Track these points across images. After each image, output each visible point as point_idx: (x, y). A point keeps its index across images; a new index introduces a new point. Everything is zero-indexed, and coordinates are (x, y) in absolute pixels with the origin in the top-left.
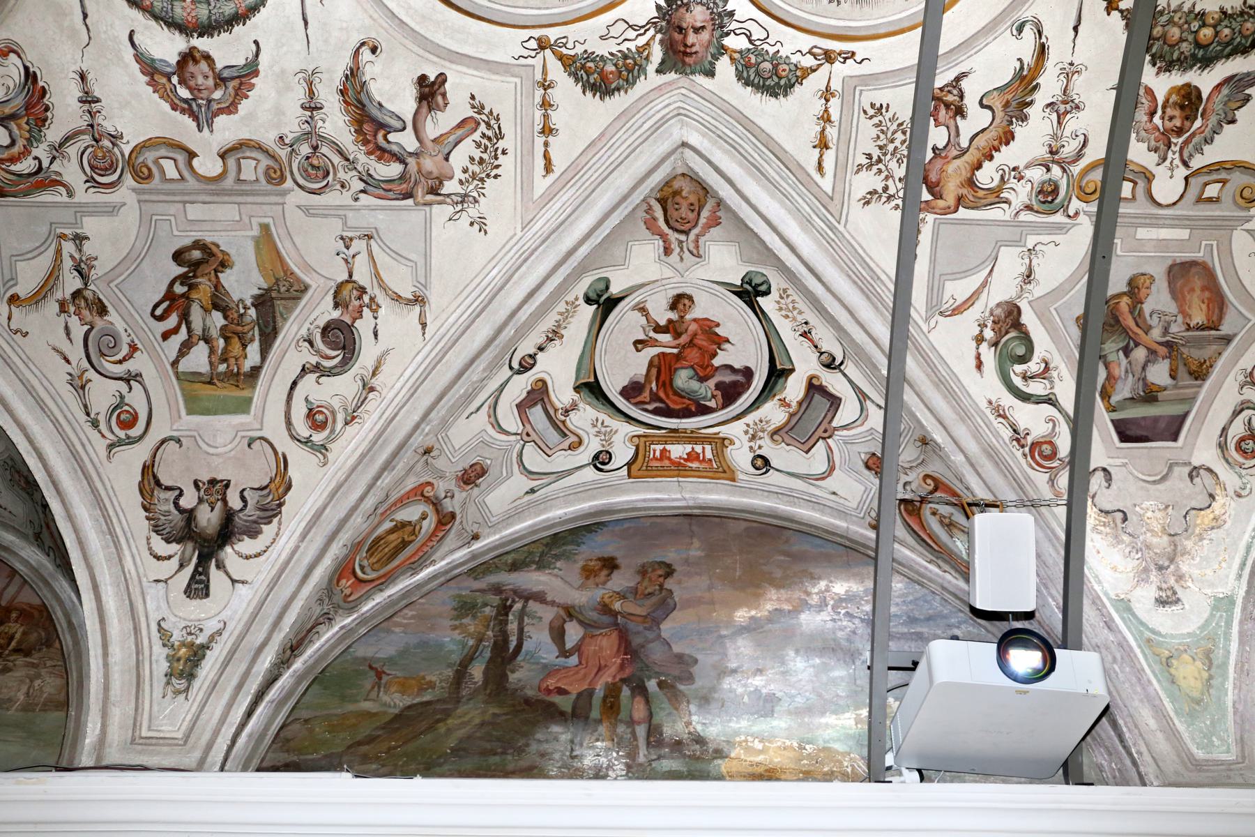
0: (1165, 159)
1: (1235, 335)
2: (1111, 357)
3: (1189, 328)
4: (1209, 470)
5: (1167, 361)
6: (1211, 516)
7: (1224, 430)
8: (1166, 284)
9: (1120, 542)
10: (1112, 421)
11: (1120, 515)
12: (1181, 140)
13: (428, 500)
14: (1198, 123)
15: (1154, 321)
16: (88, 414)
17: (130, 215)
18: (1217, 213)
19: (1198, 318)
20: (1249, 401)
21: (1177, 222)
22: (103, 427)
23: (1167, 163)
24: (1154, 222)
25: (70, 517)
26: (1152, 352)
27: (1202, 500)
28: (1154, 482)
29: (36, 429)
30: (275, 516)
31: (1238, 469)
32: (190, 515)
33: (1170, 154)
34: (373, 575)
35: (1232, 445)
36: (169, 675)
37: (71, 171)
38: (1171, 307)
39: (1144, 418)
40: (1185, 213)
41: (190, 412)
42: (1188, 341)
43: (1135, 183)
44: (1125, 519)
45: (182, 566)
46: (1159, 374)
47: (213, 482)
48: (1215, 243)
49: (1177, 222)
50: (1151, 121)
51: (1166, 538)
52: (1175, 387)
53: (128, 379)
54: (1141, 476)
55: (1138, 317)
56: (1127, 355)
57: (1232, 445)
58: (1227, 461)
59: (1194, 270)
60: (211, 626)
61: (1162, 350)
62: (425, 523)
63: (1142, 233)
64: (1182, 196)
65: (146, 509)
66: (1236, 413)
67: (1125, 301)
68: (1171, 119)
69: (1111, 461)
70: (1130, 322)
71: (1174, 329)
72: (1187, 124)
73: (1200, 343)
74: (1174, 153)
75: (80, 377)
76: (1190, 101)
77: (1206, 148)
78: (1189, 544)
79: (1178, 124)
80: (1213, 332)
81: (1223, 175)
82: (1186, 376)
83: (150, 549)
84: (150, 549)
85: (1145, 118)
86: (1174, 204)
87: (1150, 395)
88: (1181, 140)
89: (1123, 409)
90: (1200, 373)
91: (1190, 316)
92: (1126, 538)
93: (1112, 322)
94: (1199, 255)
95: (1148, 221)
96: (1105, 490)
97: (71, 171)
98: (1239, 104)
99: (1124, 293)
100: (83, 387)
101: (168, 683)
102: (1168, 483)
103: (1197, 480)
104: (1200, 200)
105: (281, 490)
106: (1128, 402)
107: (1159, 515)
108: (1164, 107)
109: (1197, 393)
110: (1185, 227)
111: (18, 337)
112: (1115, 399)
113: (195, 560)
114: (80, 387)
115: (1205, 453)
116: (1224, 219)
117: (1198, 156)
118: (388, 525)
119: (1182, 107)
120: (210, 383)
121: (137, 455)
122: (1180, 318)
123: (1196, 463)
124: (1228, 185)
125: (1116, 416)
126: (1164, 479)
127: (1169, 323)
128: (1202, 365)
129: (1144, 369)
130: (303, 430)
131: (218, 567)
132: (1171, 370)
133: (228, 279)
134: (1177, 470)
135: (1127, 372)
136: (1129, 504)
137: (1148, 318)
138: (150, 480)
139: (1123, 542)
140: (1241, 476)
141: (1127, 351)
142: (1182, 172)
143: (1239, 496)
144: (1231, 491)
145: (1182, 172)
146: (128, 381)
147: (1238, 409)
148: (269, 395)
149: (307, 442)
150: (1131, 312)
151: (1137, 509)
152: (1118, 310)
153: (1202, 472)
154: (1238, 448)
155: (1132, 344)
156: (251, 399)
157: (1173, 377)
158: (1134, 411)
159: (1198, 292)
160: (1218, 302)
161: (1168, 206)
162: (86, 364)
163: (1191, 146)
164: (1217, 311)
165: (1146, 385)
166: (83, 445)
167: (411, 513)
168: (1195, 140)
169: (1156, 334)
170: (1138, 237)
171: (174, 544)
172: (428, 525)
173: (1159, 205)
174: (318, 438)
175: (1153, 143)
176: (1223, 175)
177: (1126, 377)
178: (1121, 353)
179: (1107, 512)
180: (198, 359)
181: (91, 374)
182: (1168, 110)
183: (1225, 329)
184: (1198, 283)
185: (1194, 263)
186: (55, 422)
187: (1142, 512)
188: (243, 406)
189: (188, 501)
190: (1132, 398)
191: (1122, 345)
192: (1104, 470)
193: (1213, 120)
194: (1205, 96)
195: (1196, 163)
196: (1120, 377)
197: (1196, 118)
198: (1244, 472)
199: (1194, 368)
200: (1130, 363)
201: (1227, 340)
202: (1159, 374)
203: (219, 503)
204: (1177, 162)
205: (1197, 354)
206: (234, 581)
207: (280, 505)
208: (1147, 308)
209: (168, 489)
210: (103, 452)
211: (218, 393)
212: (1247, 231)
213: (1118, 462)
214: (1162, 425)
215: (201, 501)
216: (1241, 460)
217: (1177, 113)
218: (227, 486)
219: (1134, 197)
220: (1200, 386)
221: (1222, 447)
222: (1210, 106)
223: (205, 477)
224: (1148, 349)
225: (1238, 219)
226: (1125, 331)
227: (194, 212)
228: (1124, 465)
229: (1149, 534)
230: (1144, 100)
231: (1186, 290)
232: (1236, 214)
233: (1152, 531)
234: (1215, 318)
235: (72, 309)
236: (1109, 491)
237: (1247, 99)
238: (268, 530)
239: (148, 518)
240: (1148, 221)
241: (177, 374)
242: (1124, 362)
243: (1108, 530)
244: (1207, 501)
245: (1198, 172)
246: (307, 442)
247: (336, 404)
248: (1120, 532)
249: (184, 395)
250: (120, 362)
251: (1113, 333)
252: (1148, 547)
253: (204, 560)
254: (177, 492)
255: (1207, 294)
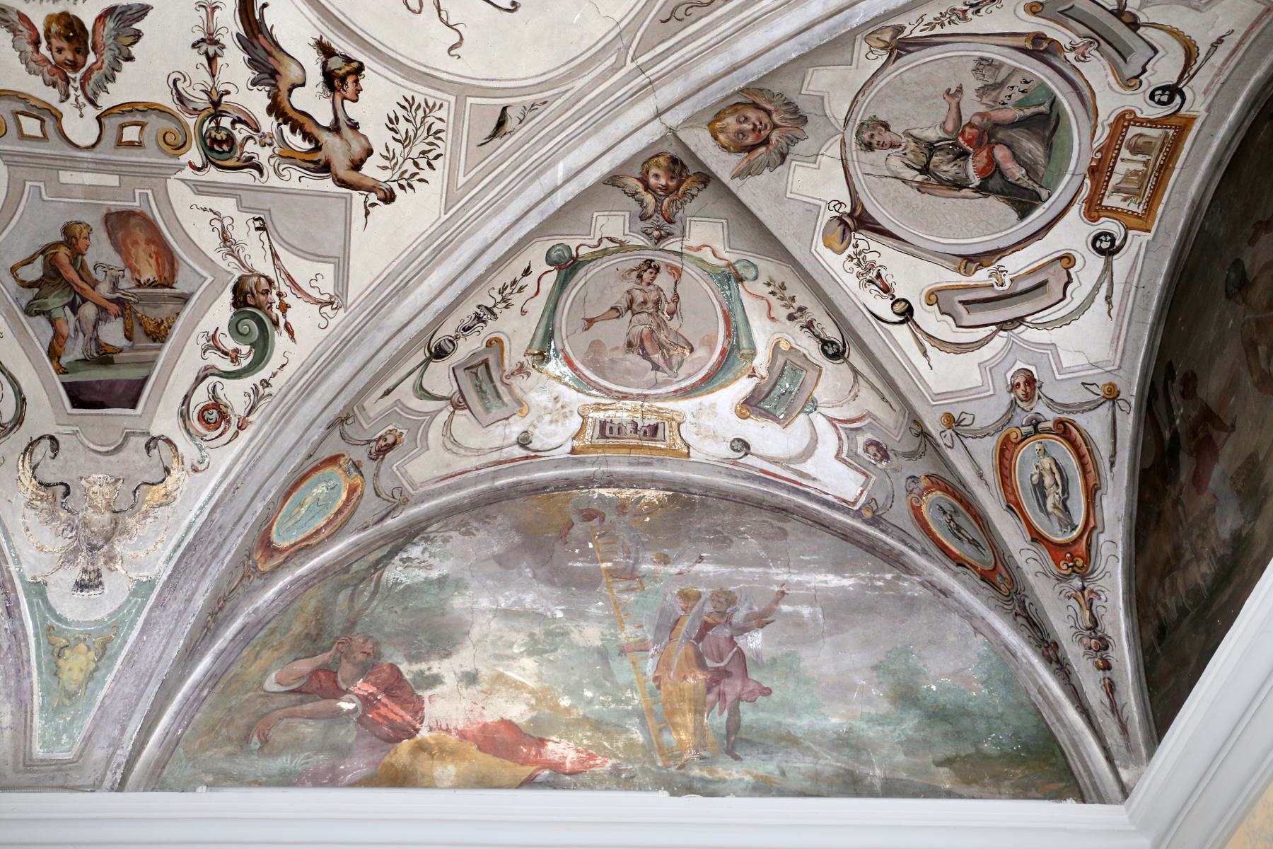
0: (68, 96)
1: (192, 294)
2: (57, 313)
3: (139, 285)
4: (168, 441)
5: (120, 321)
6: (163, 492)
7: (187, 398)
8: (104, 235)
9: (53, 516)
10: (63, 384)
11: (62, 488)
12: (78, 75)
14: (91, 58)
15: (100, 276)
18: (144, 159)
19: (148, 274)
20: (213, 367)
21: (101, 167)
23: (72, 98)
24: (74, 165)
26: (101, 309)
27: (158, 474)
28: (107, 453)
31: (198, 441)
33: (72, 91)
35: (194, 415)
38: (116, 261)
39: (99, 382)
40: (107, 157)
42: (141, 299)
43: (43, 121)
44: (67, 493)
46: (112, 333)
48: (149, 192)
49: (102, 167)
50: (38, 52)
51: (108, 515)
52: (132, 348)
54: (92, 446)
55: (82, 270)
56: (74, 312)
57: (194, 415)
58: (188, 432)
59: (133, 221)
61: (114, 308)
63: (66, 177)
64: (99, 138)
66: (199, 380)
67: (63, 253)
68: (60, 50)
69: (60, 429)
70: (72, 275)
71: (123, 284)
72: (80, 58)
73: (155, 302)
74: (76, 89)
76: (74, 31)
77: (110, 86)
78: (131, 522)
79: (70, 57)
80: (167, 290)
81: (139, 118)
82: (143, 337)
85: (30, 48)
86: (93, 146)
87: (104, 357)
88: (78, 75)
89: (75, 371)
90: (158, 334)
91: (139, 272)
92: (63, 514)
93: (52, 274)
94: (135, 205)
95: (68, 164)
96: (49, 460)
98: (130, 40)
99: (61, 243)
102: (122, 454)
103: (154, 452)
104: (120, 143)
106: (80, 364)
107: (106, 489)
108: (48, 38)
109: (157, 356)
110: (112, 173)
112: (65, 360)
115: (165, 422)
116: (153, 165)
117: (103, 94)
119: (68, 39)
122: (128, 273)
123: (155, 433)
124: (147, 129)
125: (69, 378)
126: (118, 449)
127: (117, 278)
128: (159, 325)
129: (95, 327)
132: (126, 330)
134: (133, 439)
135: (76, 330)
136: (74, 476)
137: (93, 272)
139: (59, 518)
140: (200, 449)
141: (74, 308)
142: (91, 112)
143: (195, 470)
144: (188, 466)
145: (91, 112)
147: (202, 375)
150: (73, 264)
151: (83, 482)
152: (56, 261)
153: (160, 443)
154: (201, 417)
155: (78, 299)
157: (129, 338)
158: (87, 373)
159: (143, 245)
160: (167, 258)
161: (87, 148)
163: (91, 82)
164: (167, 267)
165: (99, 345)
168: (95, 76)
169: (104, 289)
170: (63, 180)
173: (77, 147)
175: (48, 77)
176: (139, 118)
177: (77, 337)
178: (67, 309)
179: (47, 486)
182: (53, 40)
183: (181, 287)
184: (141, 236)
185: (131, 214)
187: (87, 486)
190: (85, 360)
191: (67, 300)
192: (52, 438)
193: (107, 56)
194: (89, 27)
195: (105, 101)
196: (69, 335)
197: (88, 52)
198: (205, 444)
199: (151, 328)
200: (79, 320)
201: (184, 299)
202: (112, 333)
204: (82, 99)
205: (154, 314)
208: (90, 259)
212: (183, 180)
213: (68, 429)
214: (120, 390)
216: (203, 431)
217: (64, 44)
219: (45, 135)
220: (160, 349)
221: (184, 416)
222: (99, 39)
224: (97, 306)
225: (169, 167)
226: (69, 285)
228: (75, 433)
229: (91, 510)
230: (21, 28)
231: (129, 241)
232: (164, 161)
233: (96, 506)
234: (167, 275)
236: (55, 462)
237: (138, 35)
240: (68, 164)
242: (72, 319)
243: (45, 505)
244: (160, 474)
245: (109, 112)
248: (58, 507)
251: (56, 286)
252: (86, 525)
255: (153, 248)
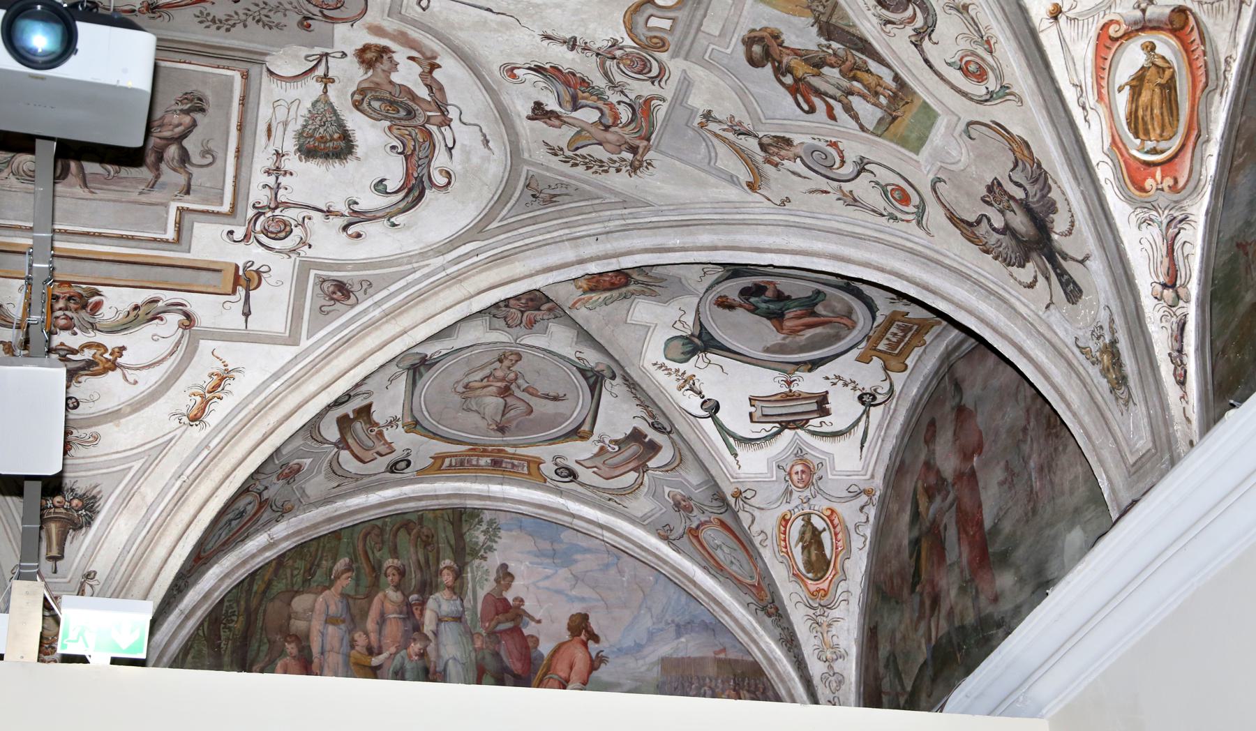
13: (1128, 35)
16: (882, 215)
17: (697, 72)
22: (899, 215)
25: (959, 306)
29: (874, 258)
30: (1046, 179)
32: (1007, 229)
34: (1175, 144)
36: (1112, 390)
37: (640, 88)
41: (917, 152)
45: (1047, 279)
47: (990, 189)
53: (862, 166)
60: (1103, 316)
62: (1161, 49)
65: (987, 252)
75: (844, 195)
83: (1020, 283)
84: (1020, 283)
97: (640, 88)
100: (855, 200)
101: (1117, 399)
105: (1026, 152)
111: (788, 206)
113: (1049, 266)
114: (854, 201)
118: (1122, 101)
120: (895, 119)
121: (935, 214)
130: (979, 90)
131: (1065, 259)
133: (791, 40)
138: (967, 228)
146: (862, 170)
148: (924, 86)
149: (991, 97)
156: (925, 102)
162: (836, 184)
166: (907, 240)
167: (1132, 59)
171: (1028, 265)
172: (1166, 46)
174: (992, 84)
180: (869, 112)
181: (847, 187)
186: (878, 240)
188: (928, 115)
189: (998, 223)
203: (1012, 203)
206: (1082, 262)
207: (1039, 166)
209: (979, 222)
210: (921, 233)
211: (907, 121)
215: (1002, 212)
218: (1000, 184)
223: (984, 192)
227: (712, 27)
235: (776, 159)
238: (1054, 194)
239: (996, 258)
241: (872, 133)
246: (991, 97)
247: (965, 45)
249: (897, 143)
250: (843, 162)
253: (1052, 258)
254: (985, 220)
